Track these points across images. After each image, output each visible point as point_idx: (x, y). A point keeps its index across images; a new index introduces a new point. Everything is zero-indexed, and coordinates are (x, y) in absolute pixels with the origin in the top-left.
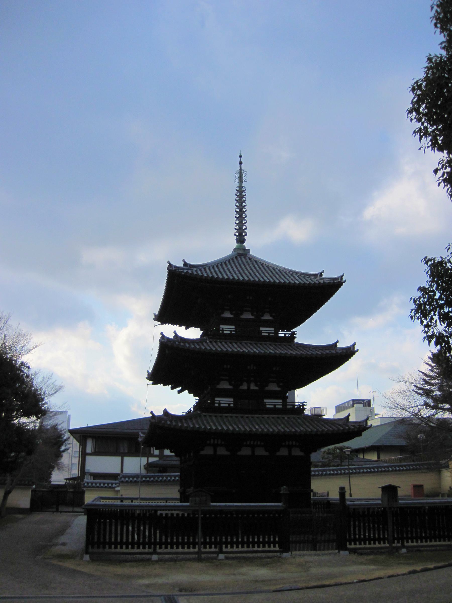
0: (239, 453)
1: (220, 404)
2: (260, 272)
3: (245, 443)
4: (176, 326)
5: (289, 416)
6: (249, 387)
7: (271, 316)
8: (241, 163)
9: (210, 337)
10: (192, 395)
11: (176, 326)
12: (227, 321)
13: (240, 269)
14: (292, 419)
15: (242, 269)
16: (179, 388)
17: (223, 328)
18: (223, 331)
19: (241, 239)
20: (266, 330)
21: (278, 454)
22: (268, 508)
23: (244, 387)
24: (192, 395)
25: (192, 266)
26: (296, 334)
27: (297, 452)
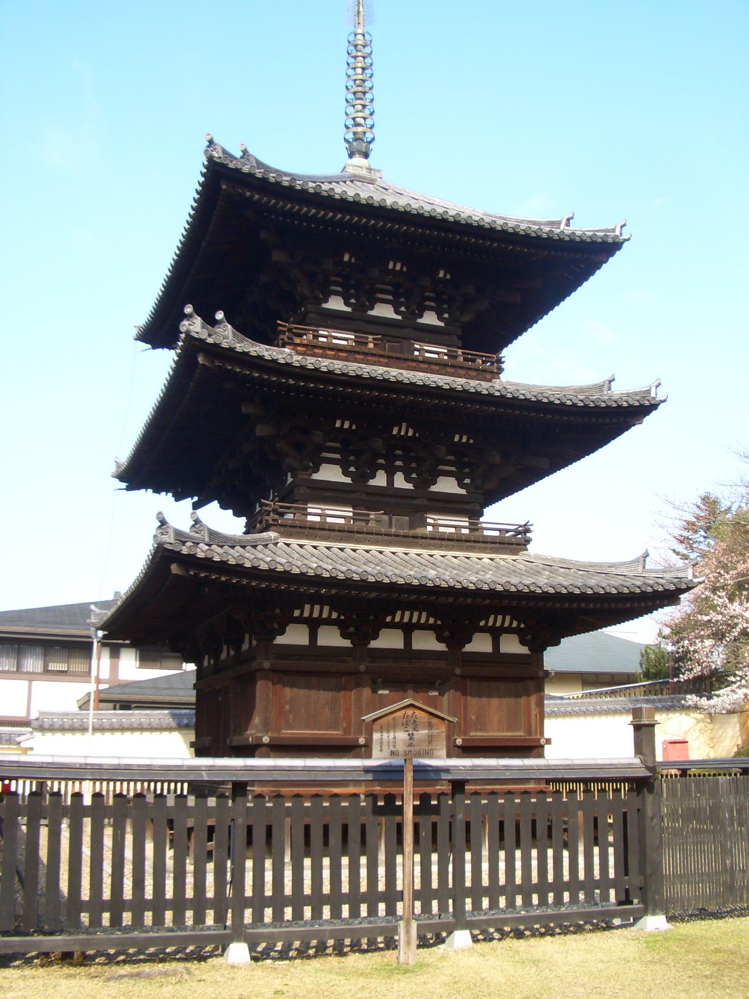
0: (374, 644)
3: (389, 619)
5: (493, 556)
6: (390, 481)
9: (299, 348)
10: (230, 512)
12: (336, 320)
14: (503, 563)
16: (196, 499)
23: (380, 480)
24: (230, 512)
27: (511, 646)
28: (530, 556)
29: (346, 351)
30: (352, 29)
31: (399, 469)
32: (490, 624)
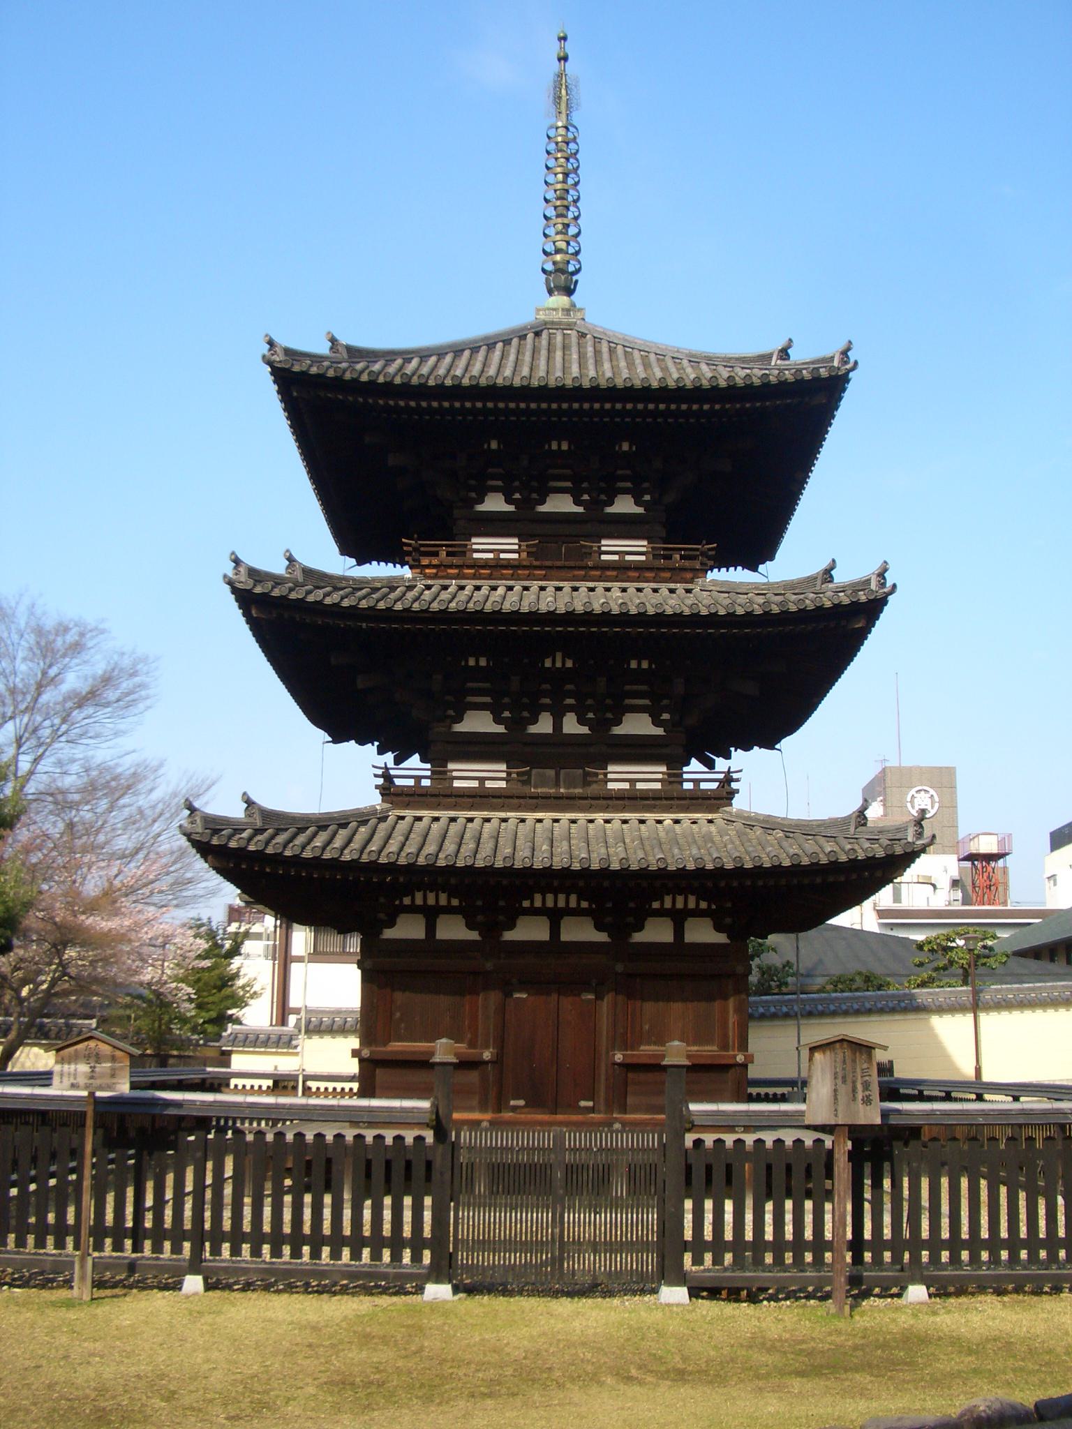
0: (509, 936)
6: (558, 725)
8: (564, 59)
9: (427, 571)
12: (495, 525)
23: (544, 725)
25: (355, 353)
27: (702, 933)
28: (730, 813)
29: (491, 567)
30: (552, 121)
31: (570, 709)
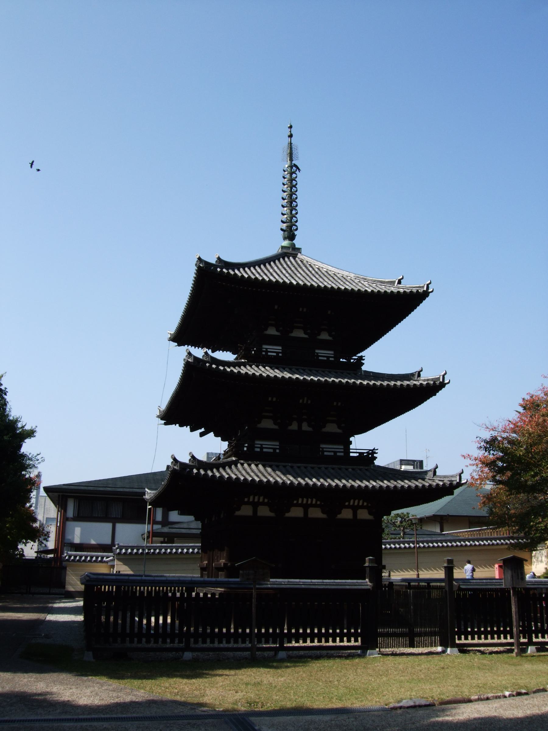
1: (262, 448)
2: (317, 276)
4: (198, 348)
5: (355, 467)
6: (300, 426)
7: (330, 335)
8: (291, 136)
10: (220, 438)
11: (198, 348)
12: (272, 341)
13: (289, 271)
14: (359, 471)
15: (292, 271)
16: (203, 430)
17: (267, 349)
18: (267, 352)
19: (290, 234)
20: (323, 354)
21: (339, 516)
22: (348, 587)
23: (294, 426)
24: (220, 438)
26: (364, 360)
27: (364, 515)
32: (351, 503)
